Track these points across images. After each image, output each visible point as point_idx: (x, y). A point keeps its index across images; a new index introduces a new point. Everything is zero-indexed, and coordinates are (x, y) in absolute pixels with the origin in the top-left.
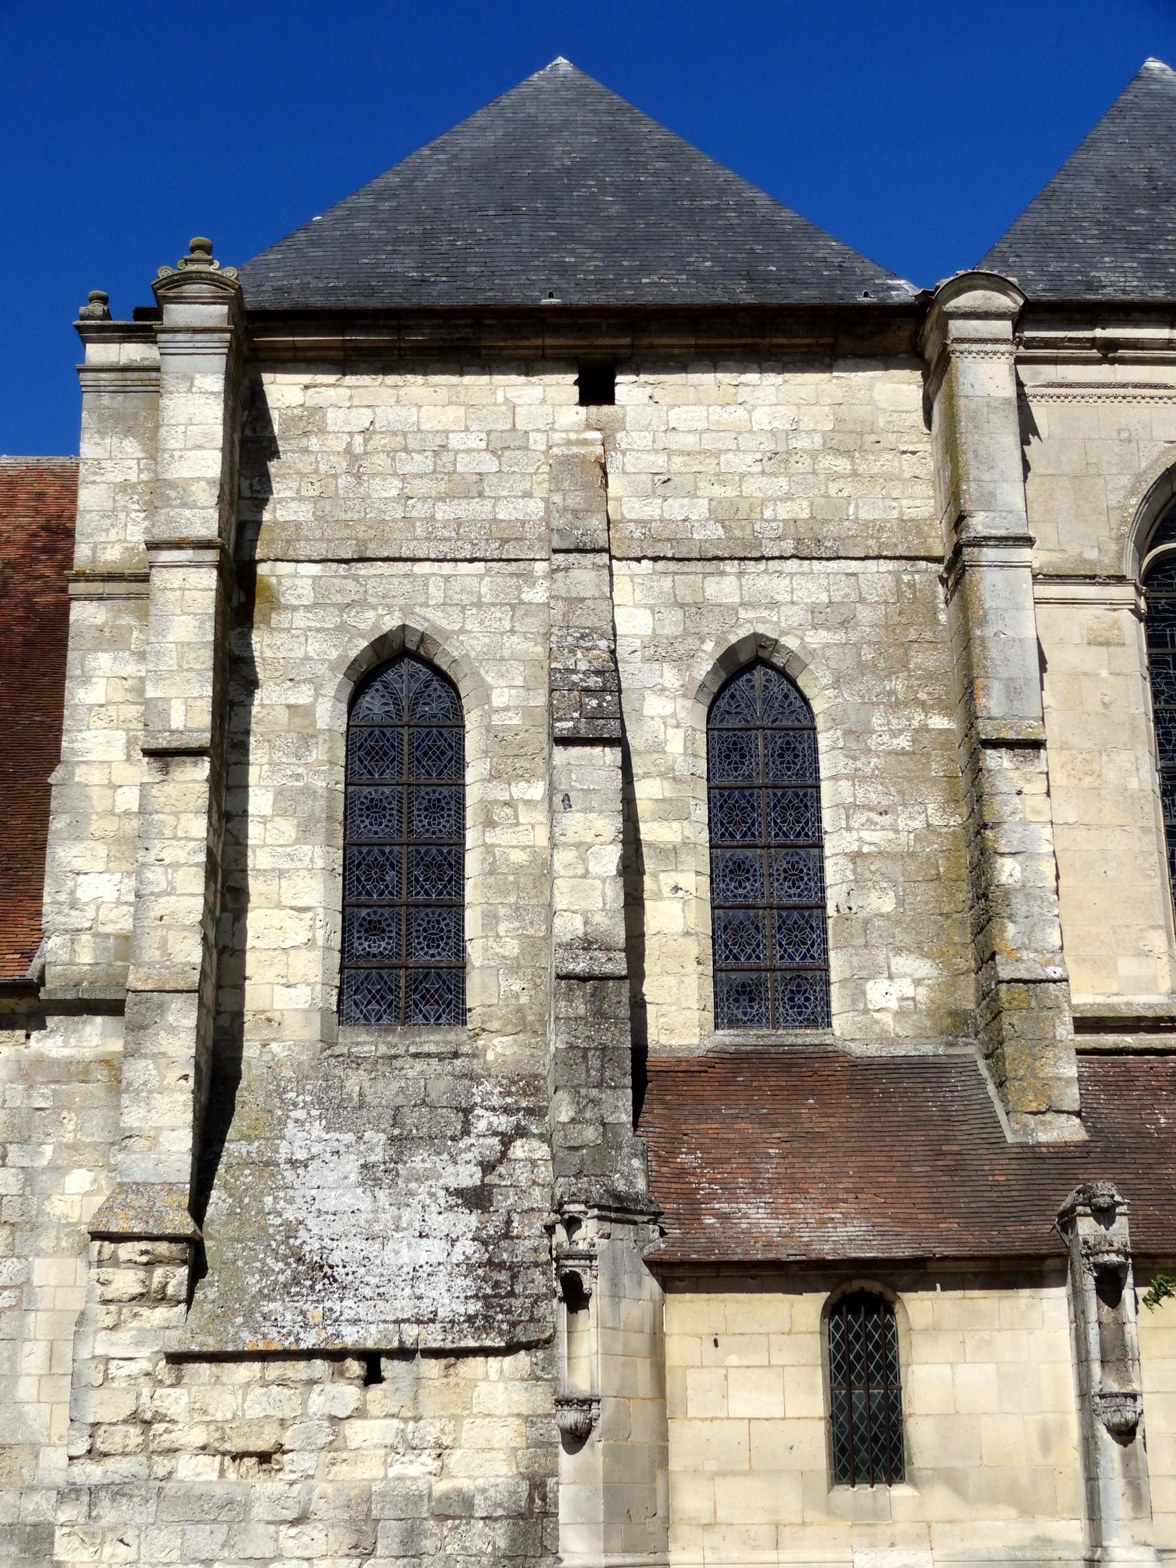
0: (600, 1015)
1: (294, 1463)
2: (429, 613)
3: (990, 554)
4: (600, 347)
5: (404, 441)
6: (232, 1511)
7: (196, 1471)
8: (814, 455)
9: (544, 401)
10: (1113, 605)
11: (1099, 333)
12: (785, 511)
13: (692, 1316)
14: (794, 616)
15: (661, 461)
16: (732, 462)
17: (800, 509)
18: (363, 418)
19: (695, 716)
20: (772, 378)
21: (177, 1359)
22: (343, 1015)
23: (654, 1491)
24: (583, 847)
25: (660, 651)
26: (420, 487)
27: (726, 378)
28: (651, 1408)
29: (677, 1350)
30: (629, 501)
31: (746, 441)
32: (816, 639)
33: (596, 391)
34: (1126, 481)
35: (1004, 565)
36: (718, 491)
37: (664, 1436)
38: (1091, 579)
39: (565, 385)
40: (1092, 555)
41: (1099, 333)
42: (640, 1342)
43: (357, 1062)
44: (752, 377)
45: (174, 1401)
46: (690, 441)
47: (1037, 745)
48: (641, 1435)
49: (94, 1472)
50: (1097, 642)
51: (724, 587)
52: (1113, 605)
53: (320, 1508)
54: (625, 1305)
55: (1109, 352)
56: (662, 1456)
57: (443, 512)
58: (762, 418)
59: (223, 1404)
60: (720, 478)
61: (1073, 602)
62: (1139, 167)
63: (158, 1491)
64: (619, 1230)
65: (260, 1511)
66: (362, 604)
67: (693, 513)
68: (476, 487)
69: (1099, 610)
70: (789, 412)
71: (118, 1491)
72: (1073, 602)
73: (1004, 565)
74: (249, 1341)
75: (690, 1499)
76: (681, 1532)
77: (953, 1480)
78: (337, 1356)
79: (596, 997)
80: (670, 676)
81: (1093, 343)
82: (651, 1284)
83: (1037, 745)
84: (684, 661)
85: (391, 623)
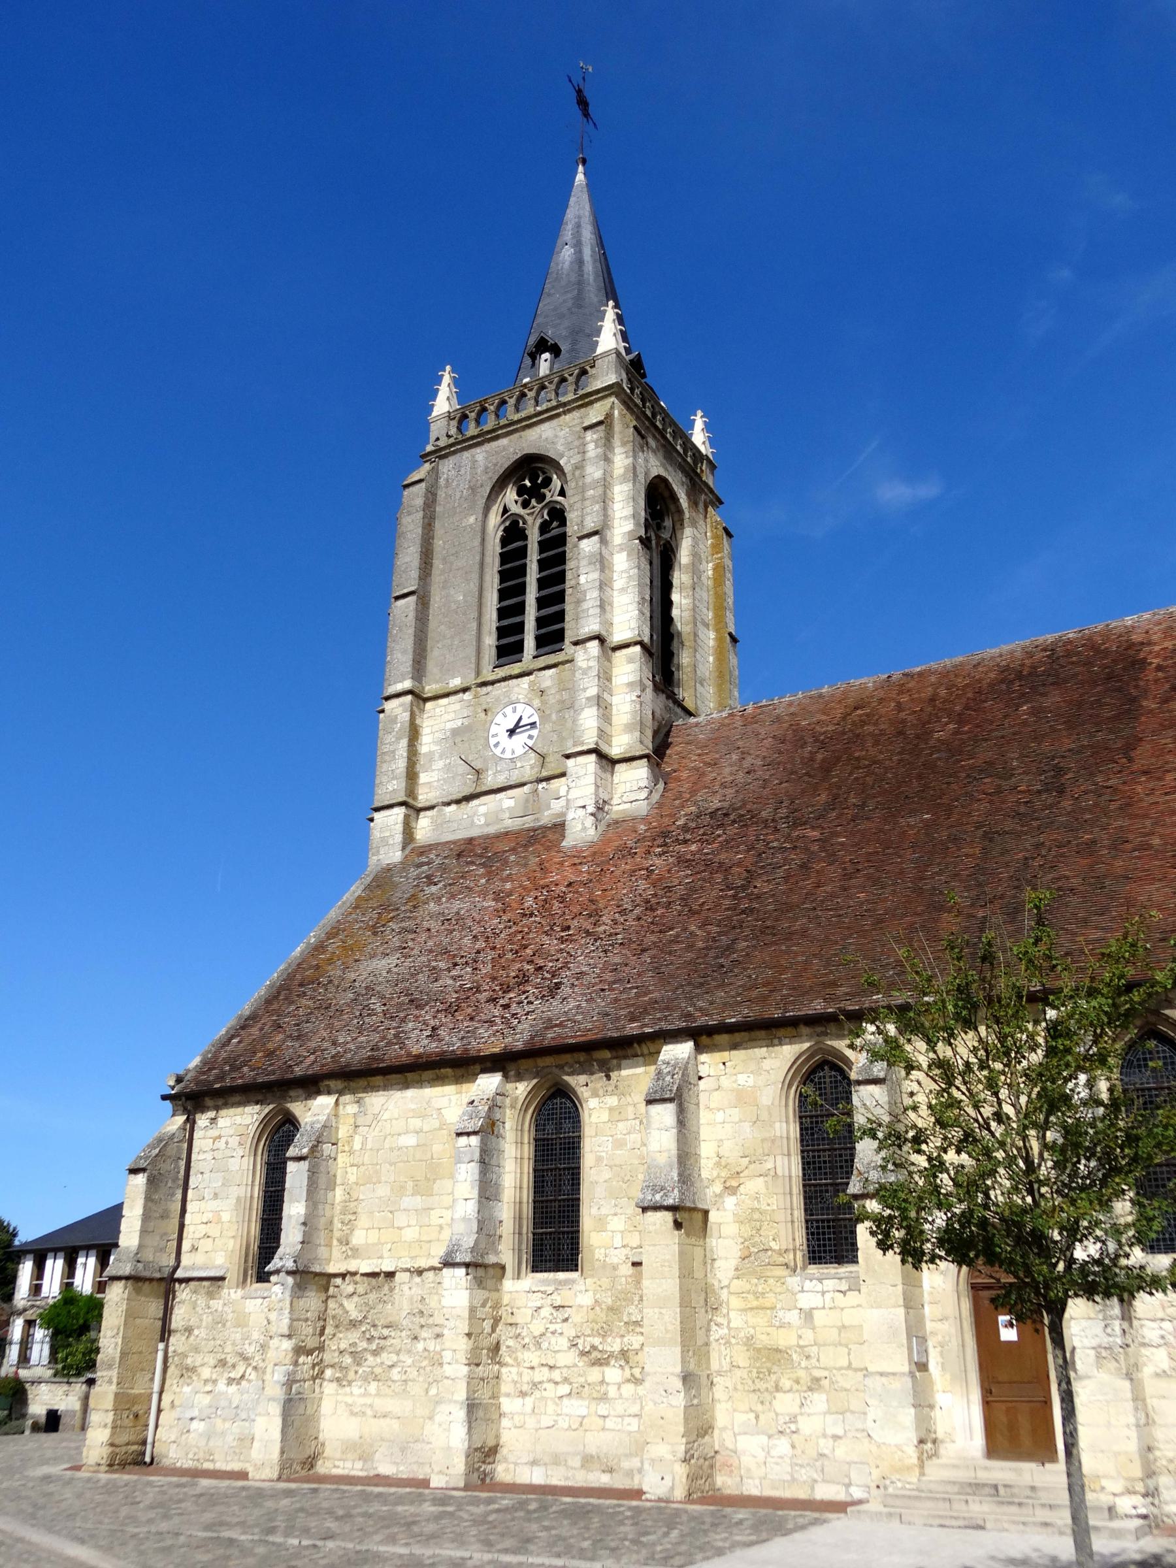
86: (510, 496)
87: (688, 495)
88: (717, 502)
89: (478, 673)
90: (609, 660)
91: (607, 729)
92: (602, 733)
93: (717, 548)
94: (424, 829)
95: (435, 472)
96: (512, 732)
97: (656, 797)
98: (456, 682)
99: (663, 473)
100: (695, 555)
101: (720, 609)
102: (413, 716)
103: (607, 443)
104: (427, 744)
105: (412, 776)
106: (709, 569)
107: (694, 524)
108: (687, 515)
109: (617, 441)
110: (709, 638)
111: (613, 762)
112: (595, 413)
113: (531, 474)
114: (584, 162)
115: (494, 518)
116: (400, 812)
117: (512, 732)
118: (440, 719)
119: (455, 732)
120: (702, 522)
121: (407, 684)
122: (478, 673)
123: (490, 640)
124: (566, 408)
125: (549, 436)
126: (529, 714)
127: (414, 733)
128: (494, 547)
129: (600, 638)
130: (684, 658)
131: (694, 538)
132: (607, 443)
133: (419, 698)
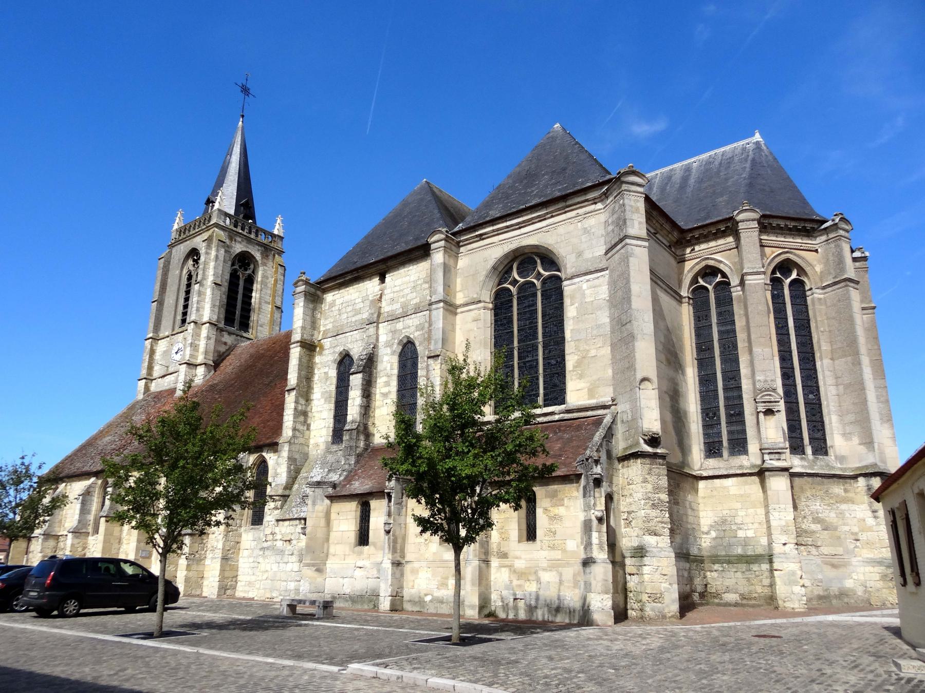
0: (351, 438)
1: (294, 542)
2: (349, 345)
3: (434, 306)
4: (381, 269)
5: (348, 304)
6: (281, 552)
7: (279, 544)
8: (421, 285)
9: (371, 286)
10: (479, 309)
11: (477, 233)
12: (414, 302)
13: (338, 507)
14: (413, 329)
15: (392, 295)
16: (406, 291)
17: (417, 300)
18: (341, 301)
19: (395, 360)
20: (415, 267)
21: (278, 521)
22: (333, 443)
23: (323, 548)
24: (354, 399)
25: (388, 345)
26: (350, 314)
27: (406, 269)
28: (325, 529)
29: (333, 516)
30: (386, 307)
31: (409, 285)
32: (417, 334)
33: (383, 280)
34: (484, 273)
35: (437, 309)
36: (402, 300)
37: (329, 535)
38: (473, 303)
39: (376, 280)
40: (475, 296)
41: (477, 233)
42: (322, 515)
43: (331, 452)
44: (411, 268)
45: (277, 530)
46: (397, 289)
47: (438, 356)
48: (320, 534)
49: (265, 545)
50: (476, 320)
51: (400, 325)
52: (479, 309)
53: (295, 552)
54: (317, 507)
55: (481, 237)
56: (327, 540)
57: (354, 319)
58: (413, 278)
59: (284, 530)
60: (403, 296)
61: (470, 310)
62: (527, 168)
63: (272, 548)
64: (317, 490)
65: (287, 553)
66: (337, 346)
67: (397, 308)
68: (357, 312)
69: (476, 311)
70: (417, 275)
71: (268, 548)
72: (470, 310)
73: (437, 309)
74: (288, 517)
75: (332, 550)
76: (330, 556)
77: (375, 545)
78: (300, 519)
79: (351, 435)
80: (389, 350)
81: (477, 236)
82: (327, 502)
83: (438, 356)
84: (391, 346)
85: (342, 349)
86: (191, 262)
87: (262, 254)
88: (281, 253)
89: (173, 330)
90: (200, 329)
91: (196, 354)
92: (191, 356)
93: (276, 272)
94: (154, 387)
95: (170, 253)
96: (176, 353)
97: (208, 377)
98: (167, 334)
99: (245, 249)
100: (265, 277)
101: (274, 297)
102: (152, 346)
103: (209, 247)
104: (158, 356)
105: (150, 368)
106: (272, 281)
107: (264, 264)
108: (260, 262)
109: (213, 246)
110: (268, 308)
111: (196, 366)
112: (205, 236)
113: (194, 254)
114: (243, 116)
115: (185, 271)
116: (144, 381)
117: (176, 353)
118: (162, 346)
119: (165, 352)
120: (271, 263)
121: (151, 335)
122: (173, 330)
123: (179, 317)
124: (203, 231)
125: (198, 242)
126: (181, 346)
127: (152, 352)
128: (184, 281)
129: (195, 323)
130: (254, 317)
131: (264, 270)
132: (209, 247)
133: (155, 339)
